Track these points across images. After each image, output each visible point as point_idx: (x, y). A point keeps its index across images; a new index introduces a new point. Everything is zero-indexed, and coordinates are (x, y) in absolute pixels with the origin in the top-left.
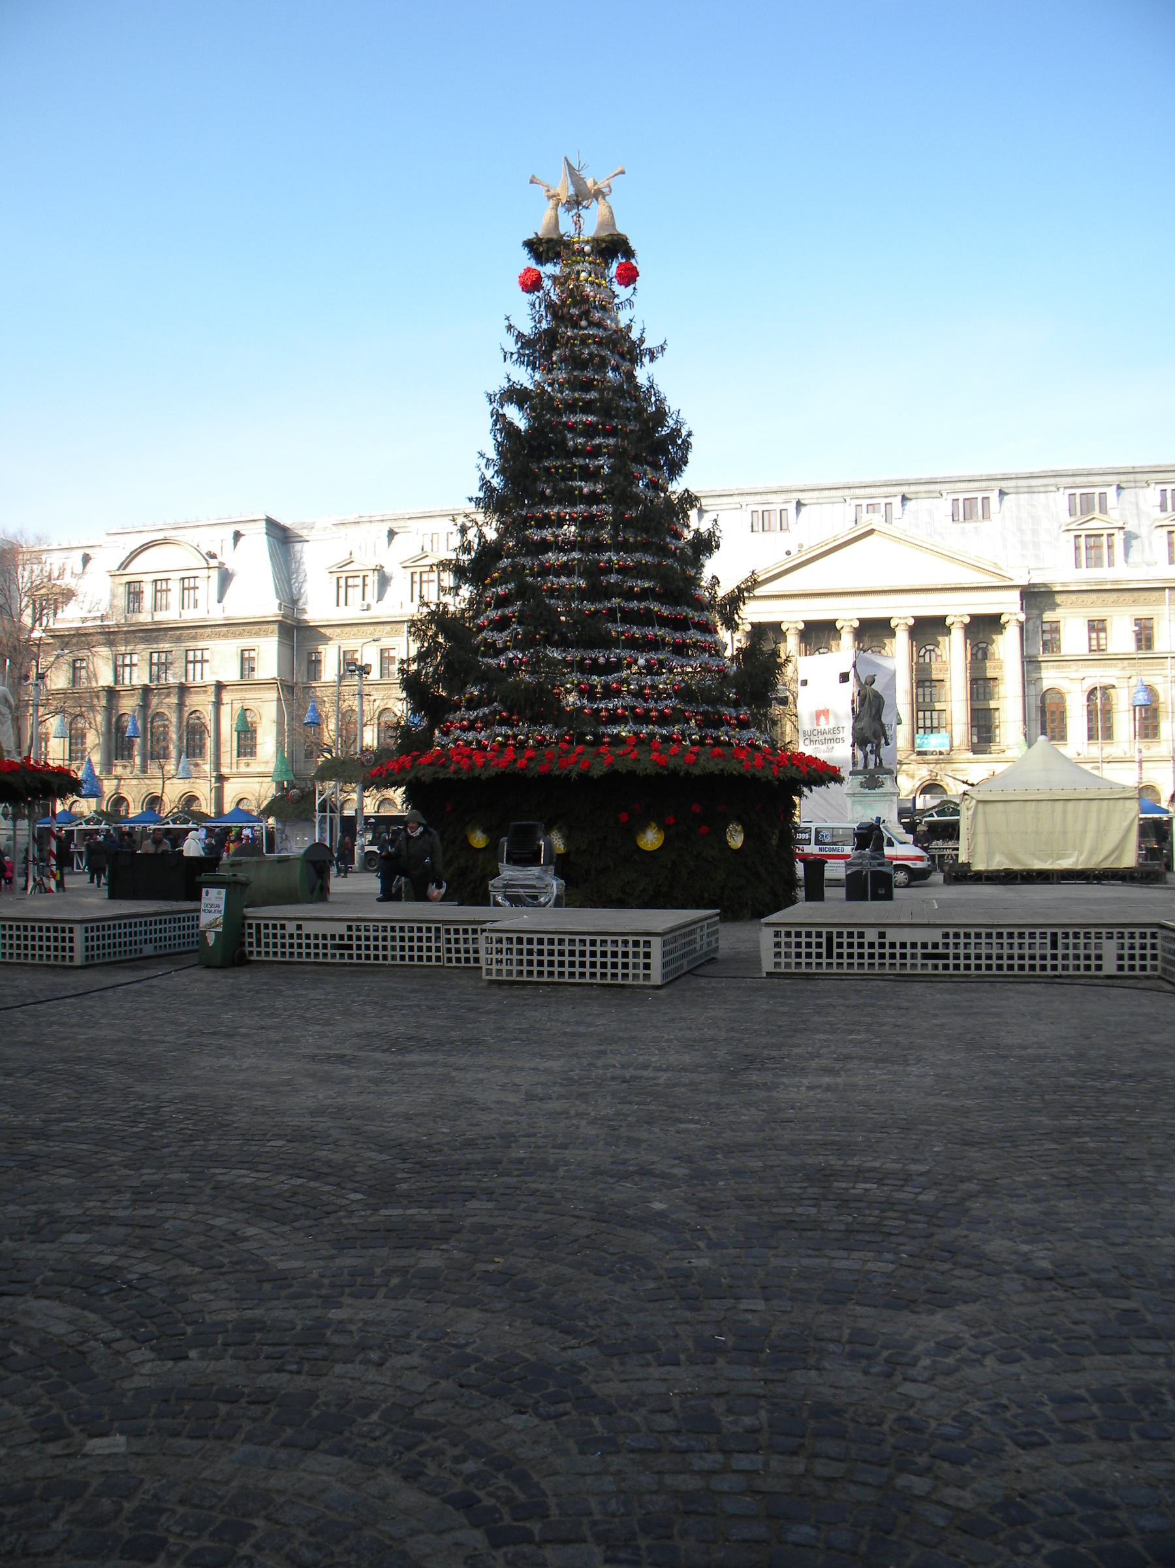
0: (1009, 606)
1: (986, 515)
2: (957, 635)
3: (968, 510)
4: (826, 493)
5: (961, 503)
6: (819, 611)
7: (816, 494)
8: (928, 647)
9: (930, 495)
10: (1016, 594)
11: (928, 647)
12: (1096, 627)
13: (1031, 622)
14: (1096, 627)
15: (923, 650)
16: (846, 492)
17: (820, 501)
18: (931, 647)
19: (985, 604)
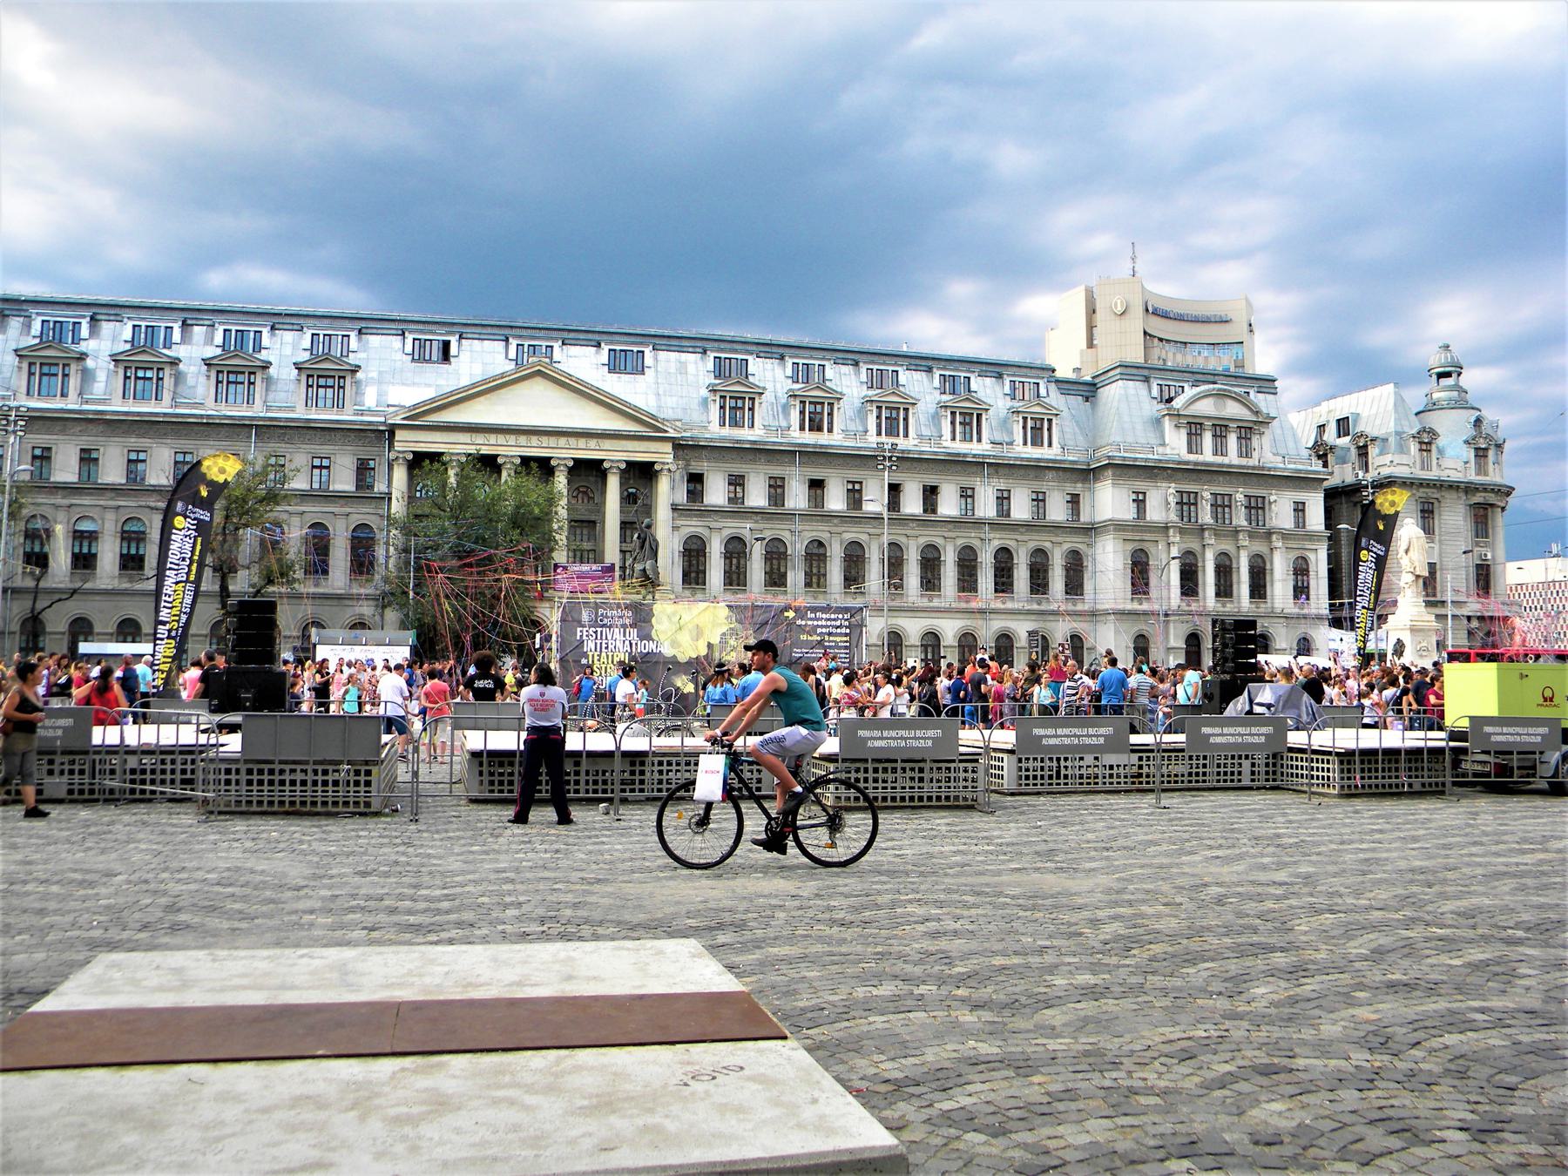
4: (489, 330)
10: (668, 447)
12: (737, 481)
14: (737, 481)
19: (641, 452)
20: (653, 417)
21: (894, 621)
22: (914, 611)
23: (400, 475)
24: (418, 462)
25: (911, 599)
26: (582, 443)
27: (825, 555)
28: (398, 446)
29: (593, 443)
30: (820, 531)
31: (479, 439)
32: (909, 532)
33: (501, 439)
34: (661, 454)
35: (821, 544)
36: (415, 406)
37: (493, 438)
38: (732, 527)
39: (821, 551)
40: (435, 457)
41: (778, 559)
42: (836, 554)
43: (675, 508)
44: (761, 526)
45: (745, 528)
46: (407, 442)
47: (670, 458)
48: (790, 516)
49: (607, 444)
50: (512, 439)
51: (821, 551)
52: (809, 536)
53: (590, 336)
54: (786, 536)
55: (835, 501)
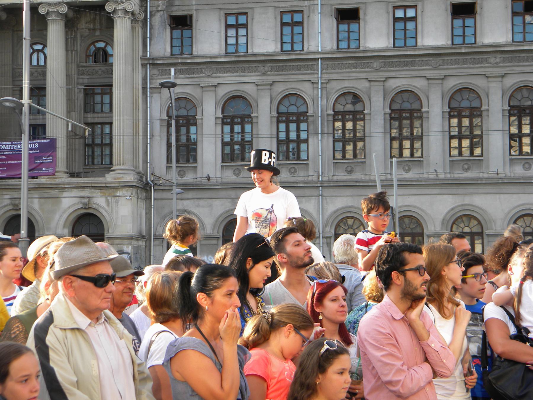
14: (236, 22)
21: (467, 200)
22: (498, 184)
25: (493, 170)
27: (362, 112)
30: (356, 81)
32: (489, 71)
35: (356, 98)
38: (231, 82)
39: (359, 107)
41: (298, 123)
42: (377, 108)
43: (150, 63)
44: (269, 79)
45: (246, 83)
48: (307, 63)
51: (359, 107)
52: (337, 87)
54: (306, 90)
55: (376, 36)
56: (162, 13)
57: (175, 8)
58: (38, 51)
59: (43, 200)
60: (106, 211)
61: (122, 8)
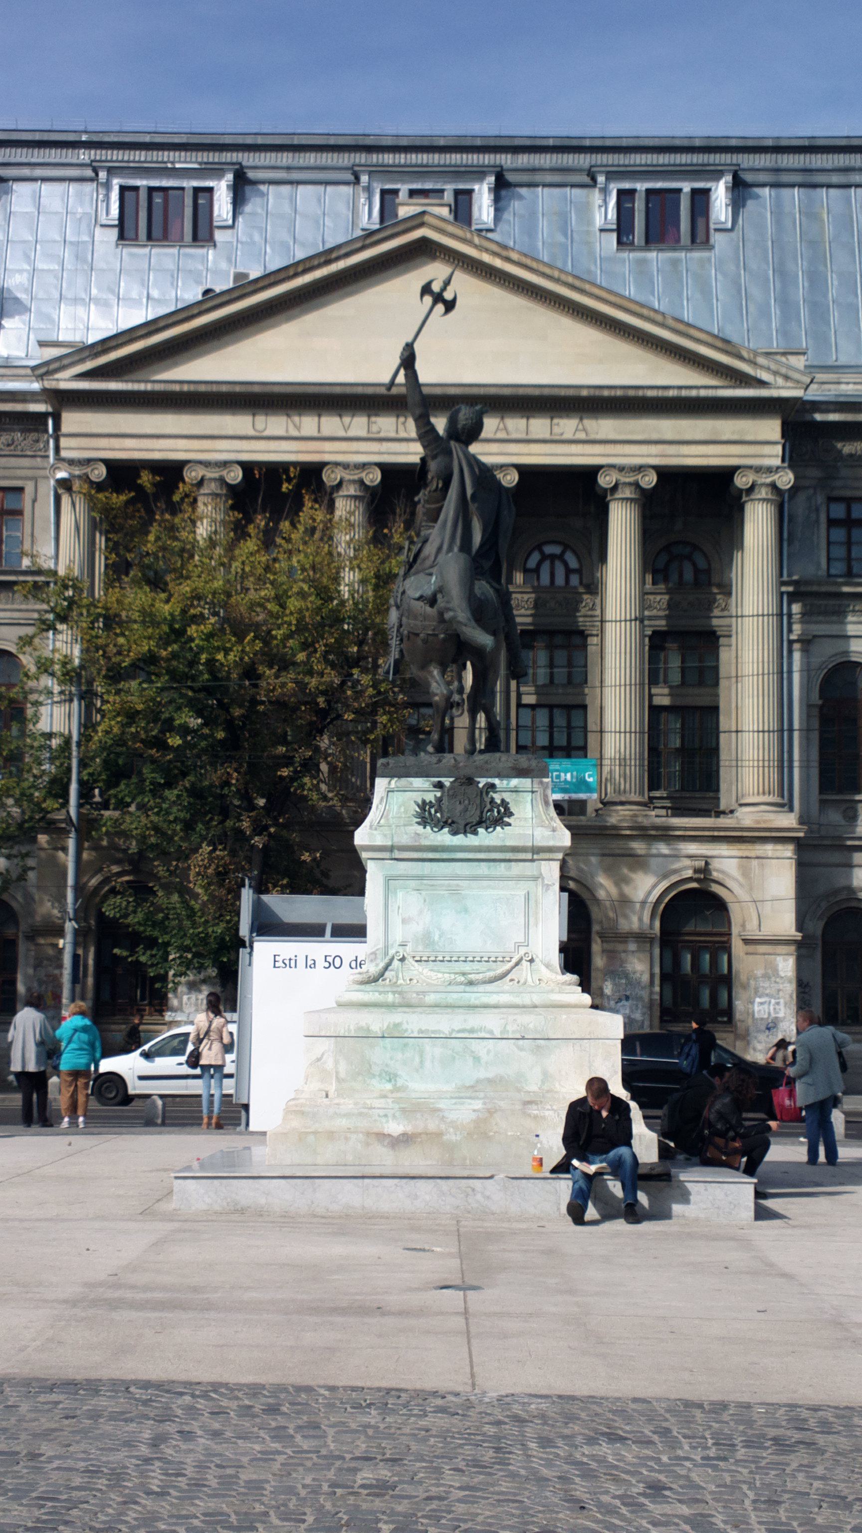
0: (754, 447)
1: (700, 238)
2: (622, 525)
3: (660, 220)
4: (311, 159)
5: (639, 205)
6: (280, 441)
7: (286, 159)
8: (549, 549)
9: (563, 179)
10: (770, 429)
11: (549, 549)
13: (801, 497)
15: (535, 558)
16: (361, 158)
17: (295, 176)
18: (555, 549)
19: (696, 443)
20: (726, 345)
23: (73, 514)
24: (137, 496)
26: (539, 426)
28: (71, 449)
29: (568, 426)
31: (276, 424)
33: (331, 424)
34: (754, 447)
36: (105, 345)
37: (308, 424)
40: (170, 472)
46: (102, 436)
47: (773, 455)
49: (606, 426)
50: (358, 424)
53: (569, 160)
56: (811, 491)
57: (838, 483)
58: (553, 557)
59: (609, 860)
60: (741, 885)
61: (769, 480)
